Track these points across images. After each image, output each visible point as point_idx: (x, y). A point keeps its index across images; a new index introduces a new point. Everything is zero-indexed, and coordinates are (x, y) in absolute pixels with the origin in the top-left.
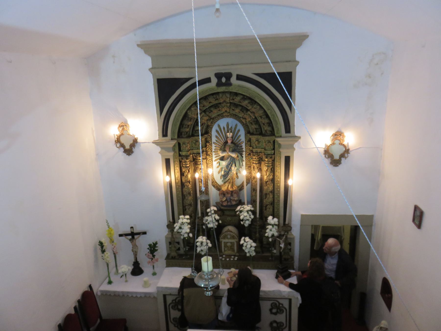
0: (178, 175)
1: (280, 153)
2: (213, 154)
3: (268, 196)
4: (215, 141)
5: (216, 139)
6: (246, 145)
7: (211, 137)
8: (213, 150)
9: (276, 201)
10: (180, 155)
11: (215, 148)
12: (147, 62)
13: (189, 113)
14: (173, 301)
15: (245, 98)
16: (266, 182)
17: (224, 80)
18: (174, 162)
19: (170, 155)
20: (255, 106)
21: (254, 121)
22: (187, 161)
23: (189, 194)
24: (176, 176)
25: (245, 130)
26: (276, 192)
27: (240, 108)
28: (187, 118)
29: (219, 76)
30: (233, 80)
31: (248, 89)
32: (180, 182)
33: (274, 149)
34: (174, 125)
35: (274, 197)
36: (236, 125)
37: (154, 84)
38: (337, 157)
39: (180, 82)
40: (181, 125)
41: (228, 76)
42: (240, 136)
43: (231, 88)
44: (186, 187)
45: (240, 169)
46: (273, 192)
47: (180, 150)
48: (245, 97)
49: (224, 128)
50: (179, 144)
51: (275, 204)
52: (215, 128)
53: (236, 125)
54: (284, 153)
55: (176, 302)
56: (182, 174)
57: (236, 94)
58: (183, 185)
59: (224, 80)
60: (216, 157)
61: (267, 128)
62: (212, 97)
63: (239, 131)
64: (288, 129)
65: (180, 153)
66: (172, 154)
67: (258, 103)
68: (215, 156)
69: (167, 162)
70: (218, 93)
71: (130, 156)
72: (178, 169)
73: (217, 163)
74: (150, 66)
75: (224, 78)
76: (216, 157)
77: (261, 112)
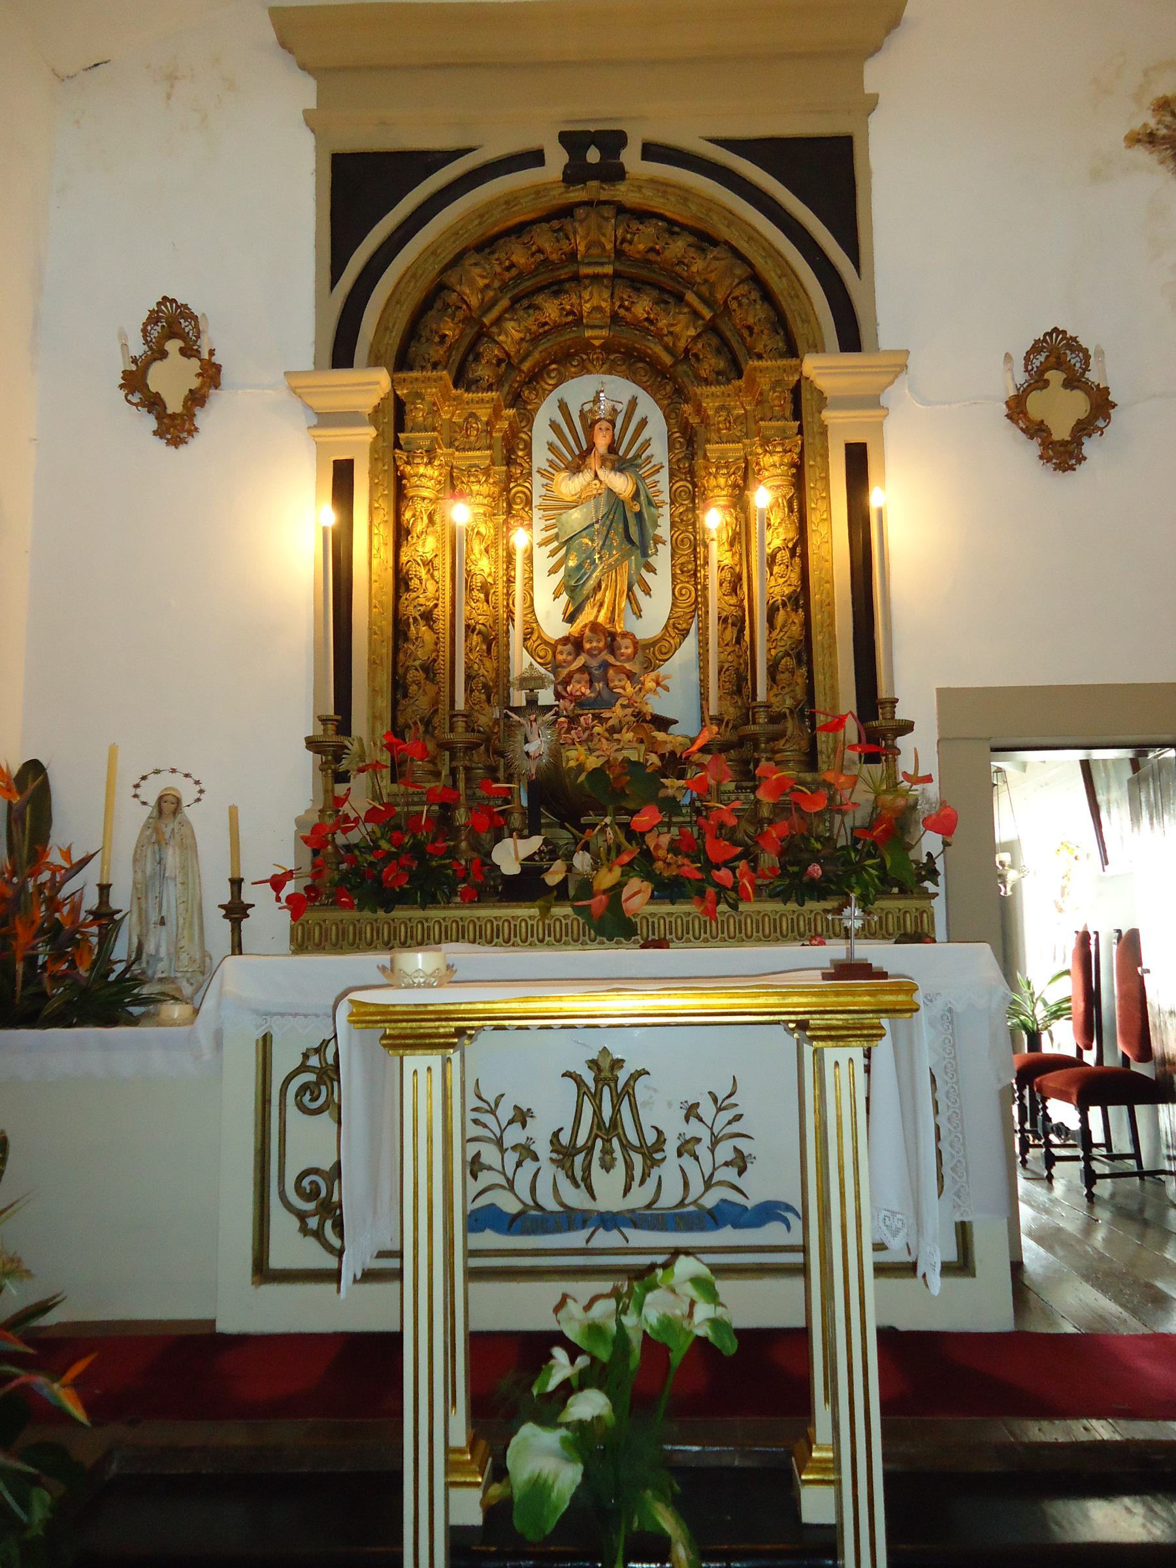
0: (385, 534)
1: (824, 431)
2: (537, 514)
3: (782, 612)
4: (546, 466)
5: (551, 457)
6: (672, 475)
7: (528, 447)
8: (536, 501)
9: (818, 638)
10: (397, 445)
11: (544, 491)
12: (304, 92)
13: (452, 278)
14: (306, 1056)
15: (673, 227)
16: (772, 560)
17: (593, 156)
18: (373, 474)
19: (358, 443)
20: (713, 252)
21: (710, 345)
22: (429, 471)
23: (428, 617)
24: (375, 539)
25: (667, 418)
26: (815, 597)
27: (655, 293)
28: (438, 305)
29: (573, 141)
30: (630, 158)
31: (686, 194)
32: (391, 563)
33: (797, 415)
34: (382, 327)
35: (807, 624)
36: (633, 403)
37: (317, 171)
38: (1061, 431)
39: (425, 162)
40: (413, 332)
41: (613, 141)
42: (647, 443)
43: (622, 187)
44: (414, 583)
45: (648, 577)
46: (800, 598)
47: (400, 425)
48: (677, 229)
49: (582, 415)
50: (400, 406)
51: (816, 648)
52: (546, 412)
53: (633, 403)
54: (842, 425)
55: (322, 1059)
56: (401, 534)
57: (643, 215)
58: (401, 580)
59: (593, 156)
60: (546, 529)
61: (766, 341)
62: (545, 226)
63: (643, 423)
64: (851, 338)
65: (401, 435)
66: (368, 433)
67: (727, 243)
68: (543, 524)
69: (343, 475)
70: (566, 212)
71: (182, 448)
72: (386, 508)
73: (553, 553)
74: (312, 104)
75: (594, 152)
76: (546, 529)
77: (740, 271)
